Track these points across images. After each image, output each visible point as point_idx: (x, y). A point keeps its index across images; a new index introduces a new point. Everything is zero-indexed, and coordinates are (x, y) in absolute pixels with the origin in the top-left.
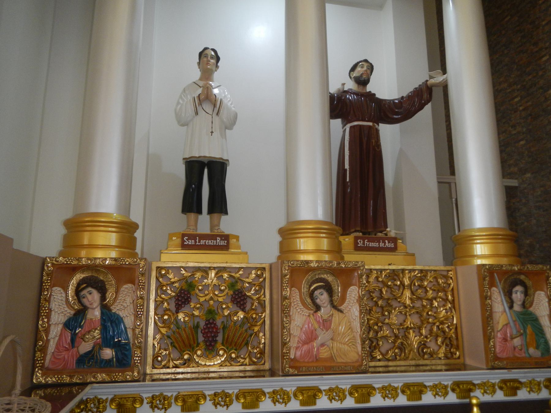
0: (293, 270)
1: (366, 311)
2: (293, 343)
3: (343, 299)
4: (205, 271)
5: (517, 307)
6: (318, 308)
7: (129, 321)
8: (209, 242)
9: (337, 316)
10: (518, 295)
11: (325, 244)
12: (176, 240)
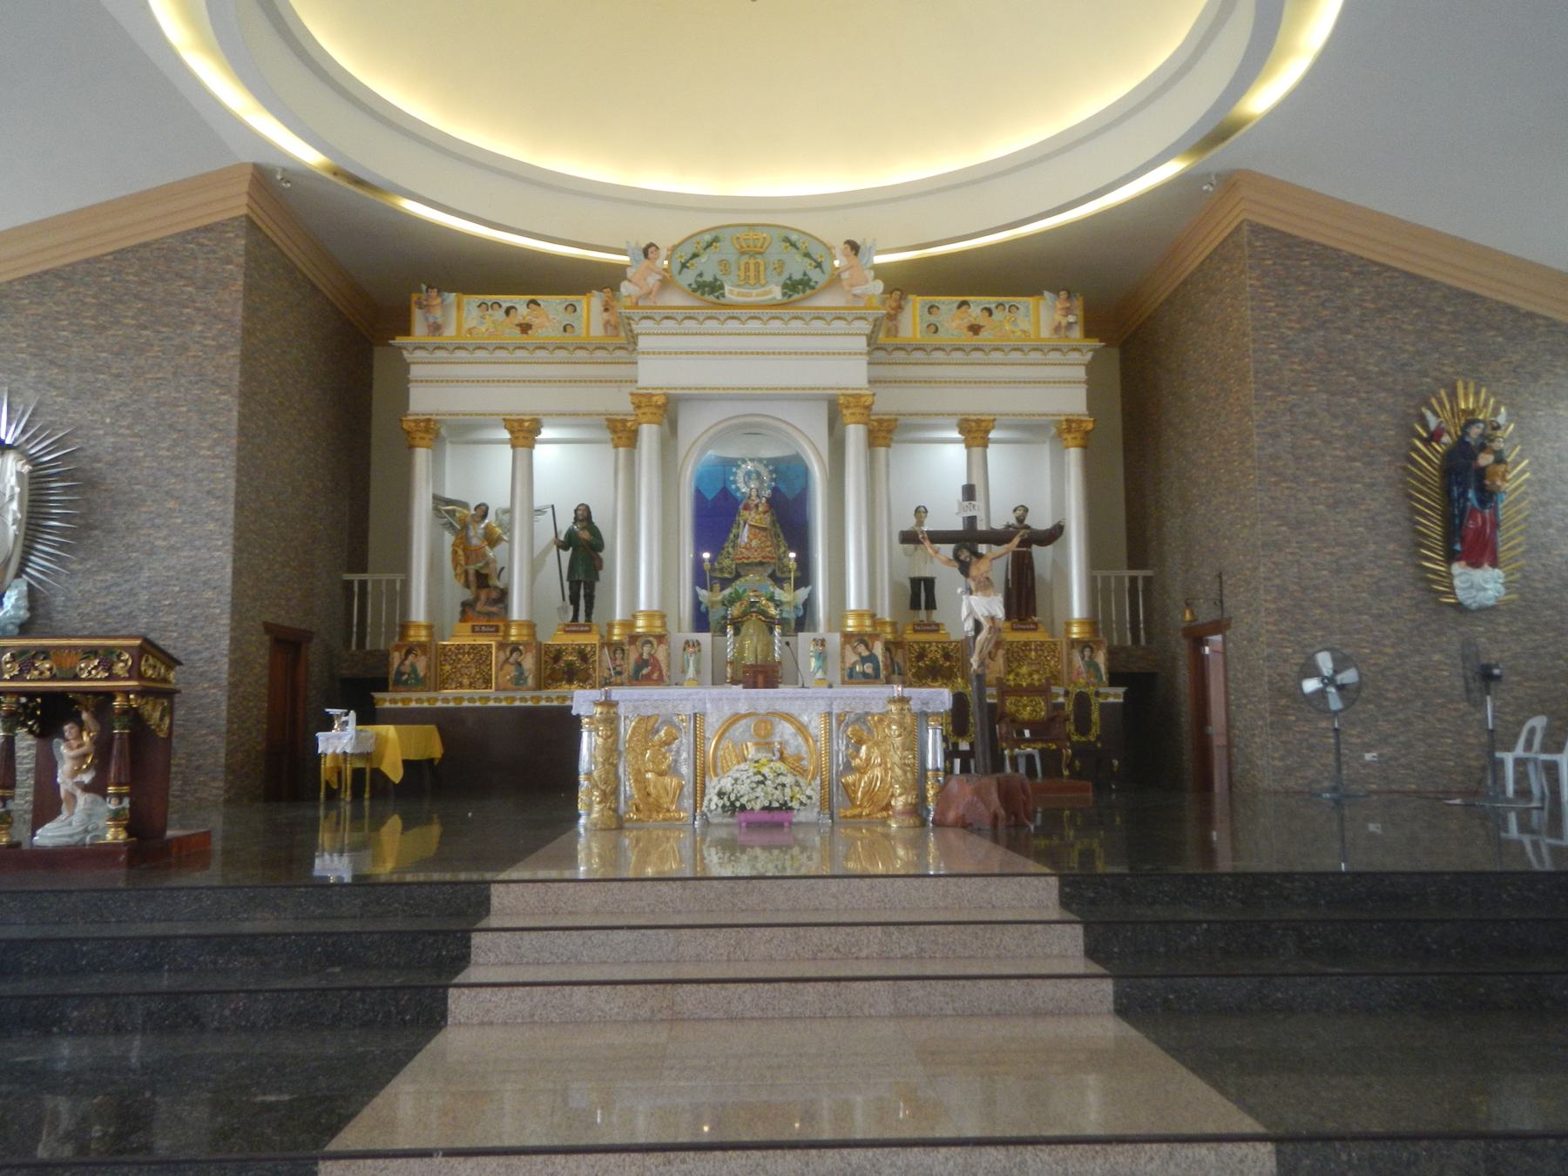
4: (930, 643)
5: (1086, 659)
8: (928, 628)
10: (1087, 652)
12: (910, 627)
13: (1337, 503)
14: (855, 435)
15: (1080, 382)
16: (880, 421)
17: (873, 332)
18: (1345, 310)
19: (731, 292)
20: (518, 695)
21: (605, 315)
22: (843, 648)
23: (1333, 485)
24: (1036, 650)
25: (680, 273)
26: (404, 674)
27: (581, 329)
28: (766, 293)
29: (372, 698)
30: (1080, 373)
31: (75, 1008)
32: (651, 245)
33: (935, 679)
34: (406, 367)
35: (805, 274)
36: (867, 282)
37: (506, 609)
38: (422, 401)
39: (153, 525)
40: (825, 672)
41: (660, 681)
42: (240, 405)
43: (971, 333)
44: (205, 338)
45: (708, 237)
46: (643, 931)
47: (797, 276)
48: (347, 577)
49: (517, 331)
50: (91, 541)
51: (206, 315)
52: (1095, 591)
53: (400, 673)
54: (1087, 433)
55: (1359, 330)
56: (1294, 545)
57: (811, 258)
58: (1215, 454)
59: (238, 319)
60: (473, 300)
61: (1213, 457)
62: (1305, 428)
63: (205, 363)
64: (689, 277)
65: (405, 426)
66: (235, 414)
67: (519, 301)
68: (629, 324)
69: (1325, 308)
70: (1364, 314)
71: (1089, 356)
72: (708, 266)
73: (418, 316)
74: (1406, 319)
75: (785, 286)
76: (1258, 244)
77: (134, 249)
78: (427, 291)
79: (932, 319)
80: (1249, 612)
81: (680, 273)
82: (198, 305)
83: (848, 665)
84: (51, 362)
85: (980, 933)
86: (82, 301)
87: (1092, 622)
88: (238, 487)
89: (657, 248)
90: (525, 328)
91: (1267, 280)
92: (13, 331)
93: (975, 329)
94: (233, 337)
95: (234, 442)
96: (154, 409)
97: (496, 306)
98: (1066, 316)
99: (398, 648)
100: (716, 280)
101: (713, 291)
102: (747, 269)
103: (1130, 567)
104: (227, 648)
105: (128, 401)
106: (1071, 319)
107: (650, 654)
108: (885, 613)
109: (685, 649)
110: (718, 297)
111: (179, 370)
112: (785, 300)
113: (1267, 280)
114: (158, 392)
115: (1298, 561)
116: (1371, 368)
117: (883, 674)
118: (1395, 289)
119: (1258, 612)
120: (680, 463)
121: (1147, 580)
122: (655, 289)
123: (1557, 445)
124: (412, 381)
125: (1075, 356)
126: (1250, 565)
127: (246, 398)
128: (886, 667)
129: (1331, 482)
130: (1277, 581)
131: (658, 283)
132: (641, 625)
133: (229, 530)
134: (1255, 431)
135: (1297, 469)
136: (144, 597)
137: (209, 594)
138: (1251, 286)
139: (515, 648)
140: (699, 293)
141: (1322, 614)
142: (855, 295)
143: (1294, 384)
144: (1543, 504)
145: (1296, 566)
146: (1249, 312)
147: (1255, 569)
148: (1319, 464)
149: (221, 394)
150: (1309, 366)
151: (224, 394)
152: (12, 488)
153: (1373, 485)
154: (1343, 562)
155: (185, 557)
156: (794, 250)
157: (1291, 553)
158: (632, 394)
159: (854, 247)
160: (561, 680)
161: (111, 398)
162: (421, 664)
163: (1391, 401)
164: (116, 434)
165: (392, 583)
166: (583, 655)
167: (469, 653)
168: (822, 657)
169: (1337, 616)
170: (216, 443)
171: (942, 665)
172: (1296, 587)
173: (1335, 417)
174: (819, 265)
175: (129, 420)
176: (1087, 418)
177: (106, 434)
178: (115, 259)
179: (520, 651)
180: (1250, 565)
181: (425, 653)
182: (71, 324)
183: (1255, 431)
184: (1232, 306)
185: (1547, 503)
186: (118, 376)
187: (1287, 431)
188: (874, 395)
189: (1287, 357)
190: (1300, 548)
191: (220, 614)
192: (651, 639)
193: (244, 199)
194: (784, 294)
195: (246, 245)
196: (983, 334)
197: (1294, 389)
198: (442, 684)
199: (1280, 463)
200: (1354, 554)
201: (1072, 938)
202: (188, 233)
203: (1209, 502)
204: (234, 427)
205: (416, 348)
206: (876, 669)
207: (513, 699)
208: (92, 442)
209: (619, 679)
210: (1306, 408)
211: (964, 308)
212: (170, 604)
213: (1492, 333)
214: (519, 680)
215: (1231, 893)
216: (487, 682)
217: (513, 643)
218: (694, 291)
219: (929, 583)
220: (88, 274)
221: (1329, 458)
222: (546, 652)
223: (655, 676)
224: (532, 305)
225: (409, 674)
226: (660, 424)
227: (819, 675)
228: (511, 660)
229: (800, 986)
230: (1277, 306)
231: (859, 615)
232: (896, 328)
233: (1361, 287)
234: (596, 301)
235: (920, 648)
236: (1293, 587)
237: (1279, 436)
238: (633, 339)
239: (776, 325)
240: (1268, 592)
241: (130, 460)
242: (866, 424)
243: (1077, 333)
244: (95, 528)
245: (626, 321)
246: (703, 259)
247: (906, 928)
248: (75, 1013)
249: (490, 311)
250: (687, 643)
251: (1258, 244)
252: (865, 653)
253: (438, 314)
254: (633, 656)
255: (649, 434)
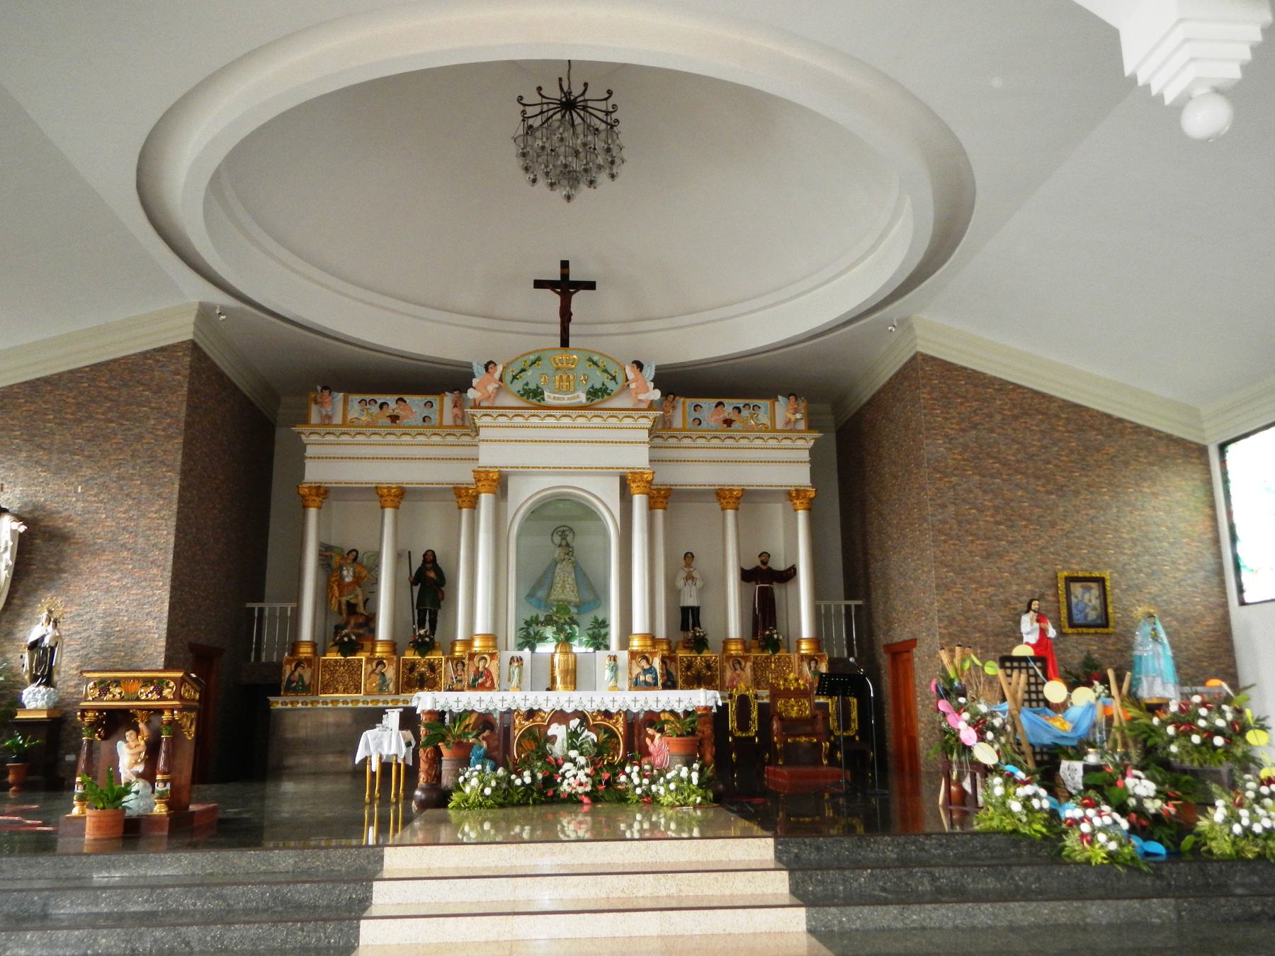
0: (727, 657)
1: (754, 670)
2: (727, 682)
3: (745, 666)
5: (812, 669)
6: (736, 670)
7: (674, 674)
9: (743, 672)
10: (813, 664)
11: (739, 647)
13: (989, 556)
14: (639, 502)
15: (805, 462)
16: (659, 490)
17: (653, 426)
18: (990, 416)
19: (549, 397)
20: (382, 698)
21: (456, 411)
22: (630, 663)
23: (985, 542)
24: (775, 662)
25: (511, 383)
26: (293, 682)
27: (435, 418)
28: (574, 398)
29: (268, 701)
30: (805, 455)
31: (104, 937)
32: (491, 362)
33: (699, 686)
34: (303, 447)
35: (603, 385)
36: (647, 390)
37: (373, 631)
38: (315, 473)
39: (109, 570)
40: (616, 681)
41: (492, 688)
42: (181, 479)
43: (725, 425)
44: (158, 430)
45: (532, 357)
46: (491, 879)
47: (598, 386)
48: (249, 605)
49: (388, 421)
50: (62, 582)
51: (158, 413)
52: (819, 617)
53: (290, 681)
54: (811, 499)
55: (1001, 430)
56: (959, 586)
57: (609, 373)
58: (903, 517)
59: (183, 415)
60: (354, 399)
61: (901, 519)
62: (964, 500)
63: (156, 448)
64: (518, 385)
65: (301, 492)
66: (177, 486)
67: (391, 399)
68: (473, 419)
69: (977, 415)
70: (1003, 419)
71: (812, 443)
72: (532, 378)
73: (314, 409)
74: (1034, 423)
75: (589, 393)
76: (927, 369)
77: (107, 364)
78: (322, 391)
79: (697, 415)
80: (929, 635)
81: (511, 383)
82: (153, 405)
83: (634, 676)
84: (38, 446)
85: (720, 878)
86: (65, 401)
87: (817, 641)
88: (176, 541)
89: (496, 365)
90: (394, 418)
91: (935, 395)
92: (10, 422)
93: (728, 422)
94: (177, 429)
95: (175, 507)
96: (115, 482)
97: (372, 402)
98: (794, 414)
99: (289, 662)
100: (538, 387)
101: (535, 397)
102: (561, 380)
103: (847, 598)
104: (163, 664)
105: (96, 476)
106: (798, 416)
107: (484, 667)
108: (661, 633)
109: (511, 664)
110: (539, 401)
111: (136, 453)
112: (589, 402)
113: (935, 395)
114: (119, 469)
115: (962, 598)
116: (1010, 457)
117: (660, 683)
118: (1025, 401)
119: (934, 636)
120: (509, 521)
121: (856, 606)
122: (493, 395)
123: (1143, 513)
124: (307, 458)
125: (800, 443)
126: (928, 600)
127: (185, 474)
128: (662, 675)
129: (984, 540)
130: (947, 613)
131: (495, 391)
132: (478, 645)
133: (168, 574)
134: (929, 503)
135: (960, 530)
136: (99, 625)
137: (151, 623)
138: (923, 398)
139: (380, 662)
140: (525, 397)
141: (979, 637)
142: (640, 400)
143: (956, 469)
144: (1137, 556)
145: (960, 601)
146: (923, 417)
147: (932, 603)
148: (975, 527)
149: (167, 471)
150: (966, 456)
151: (169, 471)
152: (7, 542)
153: (1013, 542)
154: (995, 598)
155: (133, 594)
156: (595, 367)
157: (957, 592)
158: (474, 471)
159: (639, 365)
160: (414, 687)
161: (82, 474)
162: (307, 675)
163: (1025, 481)
164: (85, 501)
165: (284, 610)
166: (432, 667)
167: (344, 666)
168: (615, 669)
169: (991, 639)
170: (161, 508)
171: (705, 674)
172: (961, 618)
173: (985, 492)
174: (614, 378)
175: (96, 490)
176: (811, 489)
177: (77, 500)
178: (91, 370)
179: (384, 664)
180: (928, 600)
181: (310, 666)
182: (55, 418)
183: (929, 503)
184: (911, 411)
185: (1138, 555)
186: (89, 457)
187: (952, 503)
188: (654, 473)
189: (951, 449)
190: (964, 589)
191: (158, 638)
192: (486, 656)
193: (191, 328)
194: (588, 399)
195: (191, 361)
196: (734, 426)
197: (955, 472)
198: (324, 690)
199: (947, 526)
200: (1002, 593)
201: (779, 883)
202: (147, 352)
203: (900, 552)
204: (176, 496)
205: (311, 433)
206: (656, 679)
207: (378, 701)
208: (67, 507)
209: (459, 686)
210: (965, 486)
211: (718, 408)
212: (119, 631)
213: (1094, 433)
214: (382, 688)
215: (890, 848)
216: (358, 690)
217: (378, 658)
218: (522, 395)
219: (695, 611)
220: (71, 381)
221: (981, 523)
222: (403, 665)
223: (488, 684)
224: (399, 402)
225: (297, 683)
226: (494, 493)
227: (612, 683)
228: (377, 671)
229: (598, 915)
230: (942, 412)
231: (644, 636)
232: (671, 423)
233: (1000, 400)
234: (448, 399)
235: (688, 660)
236: (959, 618)
237: (946, 507)
238: (476, 430)
239: (581, 421)
240: (940, 620)
241: (95, 521)
242: (647, 494)
243: (802, 425)
244: (65, 572)
245: (471, 417)
246: (529, 373)
247: (670, 875)
248: (104, 940)
249: (368, 406)
250: (512, 658)
251: (927, 369)
252: (647, 667)
253: (328, 409)
254: (472, 670)
255: (485, 500)
